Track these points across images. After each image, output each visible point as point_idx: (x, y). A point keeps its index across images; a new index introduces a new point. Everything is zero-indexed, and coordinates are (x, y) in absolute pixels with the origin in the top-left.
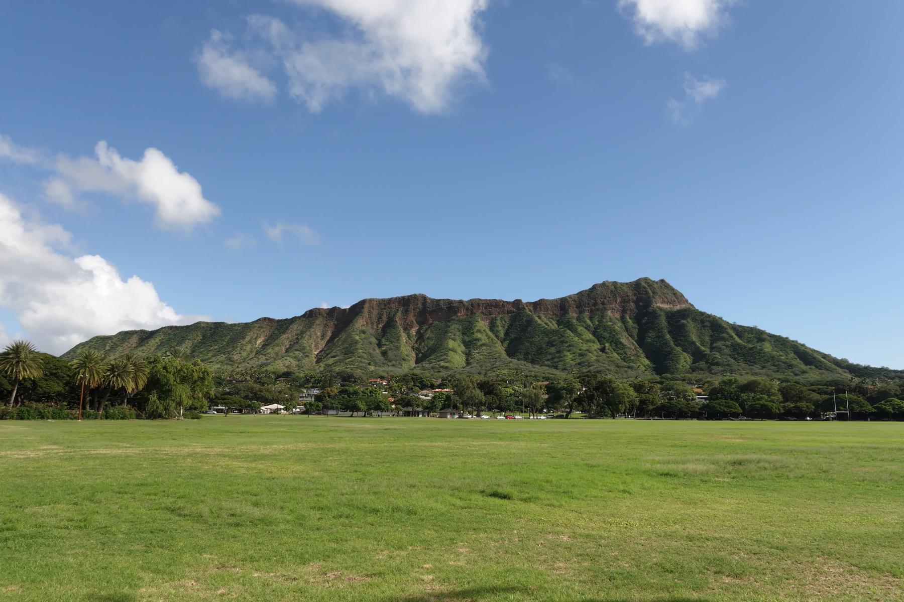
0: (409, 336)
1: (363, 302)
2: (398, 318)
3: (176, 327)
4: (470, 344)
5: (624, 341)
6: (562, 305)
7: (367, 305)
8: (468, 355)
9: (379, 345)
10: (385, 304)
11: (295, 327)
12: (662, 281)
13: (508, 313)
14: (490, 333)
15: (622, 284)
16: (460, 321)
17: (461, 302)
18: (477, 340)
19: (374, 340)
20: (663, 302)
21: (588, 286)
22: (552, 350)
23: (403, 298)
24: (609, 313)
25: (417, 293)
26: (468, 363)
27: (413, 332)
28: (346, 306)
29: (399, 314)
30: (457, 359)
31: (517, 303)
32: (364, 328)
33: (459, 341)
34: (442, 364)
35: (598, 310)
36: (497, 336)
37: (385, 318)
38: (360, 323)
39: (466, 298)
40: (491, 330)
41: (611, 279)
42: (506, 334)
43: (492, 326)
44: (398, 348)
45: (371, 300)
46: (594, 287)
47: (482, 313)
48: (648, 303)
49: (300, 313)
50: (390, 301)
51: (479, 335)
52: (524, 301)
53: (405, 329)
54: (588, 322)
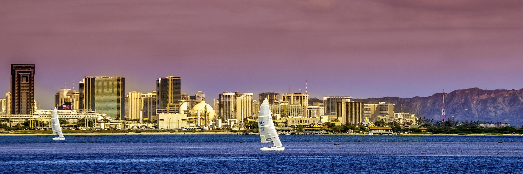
1: (455, 91)
4: (496, 108)
8: (495, 113)
17: (492, 91)
23: (470, 89)
31: (513, 90)
42: (509, 103)
44: (472, 110)
45: (458, 90)
49: (431, 95)
50: (466, 90)
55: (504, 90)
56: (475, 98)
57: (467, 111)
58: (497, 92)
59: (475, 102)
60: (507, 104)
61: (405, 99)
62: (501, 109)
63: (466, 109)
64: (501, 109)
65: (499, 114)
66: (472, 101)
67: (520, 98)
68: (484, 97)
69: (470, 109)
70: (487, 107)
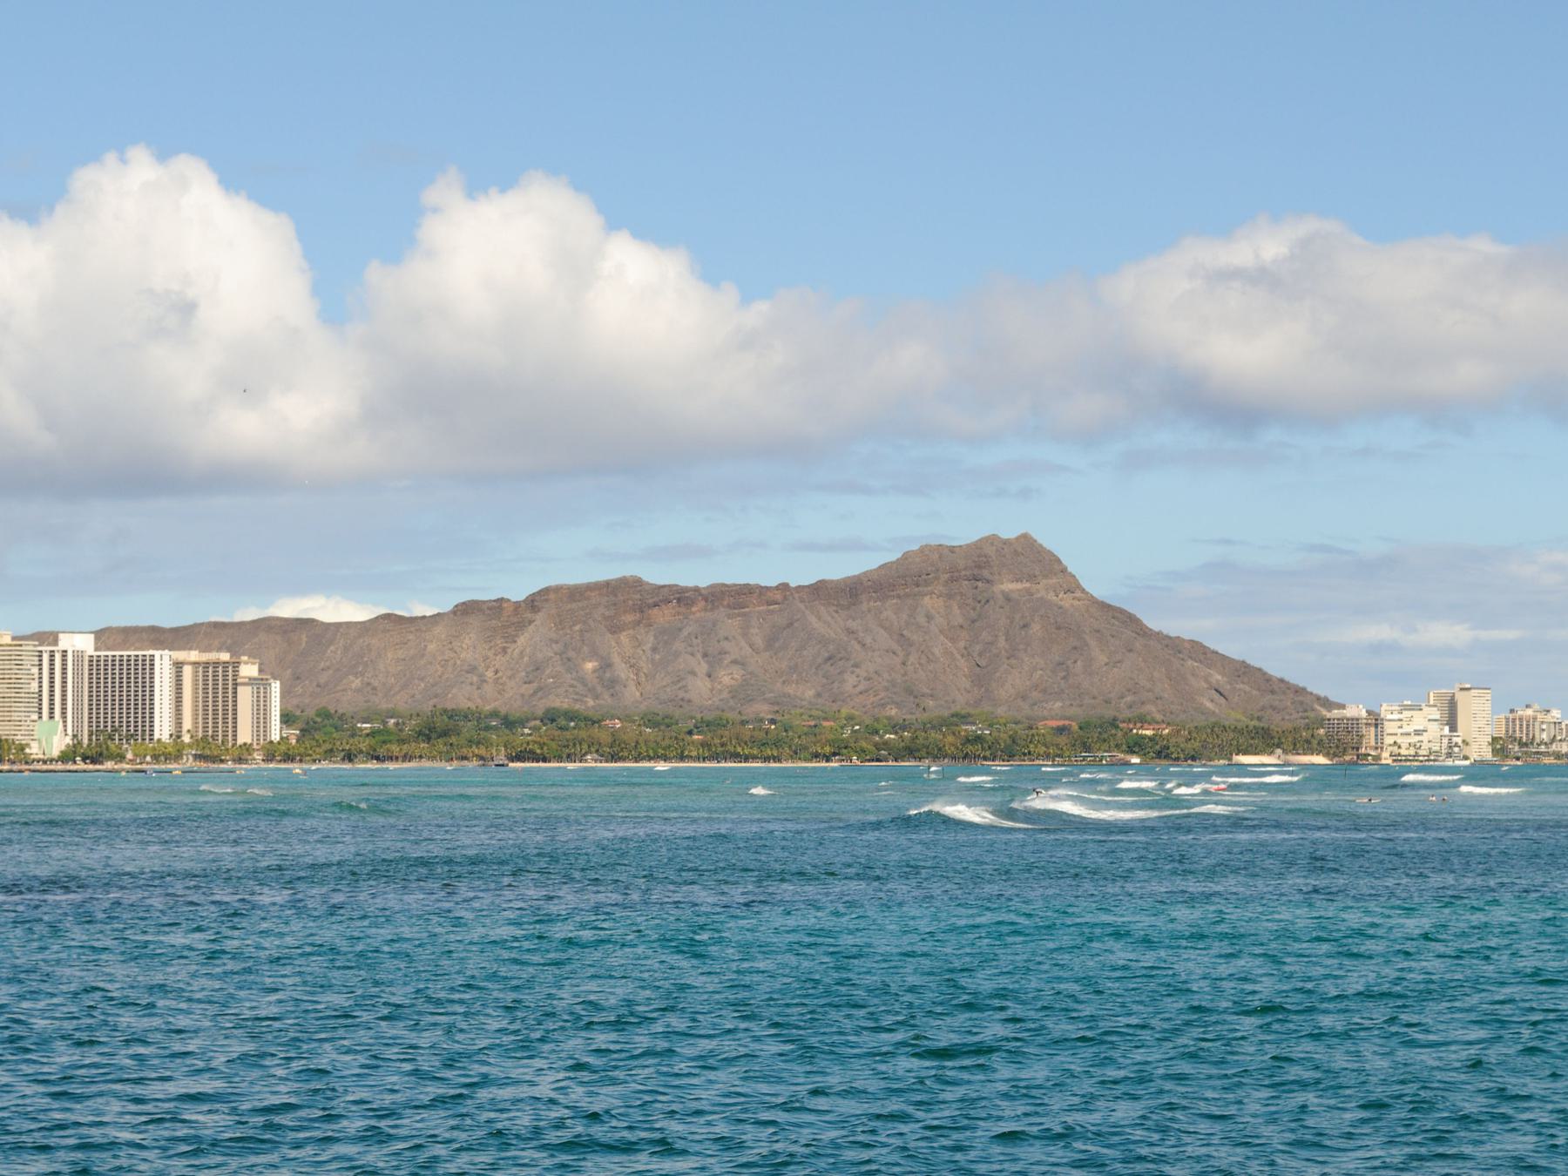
1: (545, 591)
4: (714, 660)
7: (552, 596)
10: (576, 593)
12: (1025, 537)
13: (769, 604)
14: (743, 643)
15: (952, 549)
17: (696, 590)
18: (723, 652)
23: (607, 584)
24: (927, 599)
31: (784, 587)
32: (553, 636)
33: (699, 656)
34: (681, 694)
35: (907, 595)
40: (745, 635)
42: (770, 642)
45: (557, 589)
47: (729, 606)
51: (725, 644)
52: (793, 585)
53: (613, 633)
56: (629, 618)
57: (594, 671)
59: (624, 637)
60: (759, 641)
61: (340, 624)
62: (735, 662)
63: (589, 666)
64: (735, 662)
65: (726, 680)
66: (615, 630)
67: (813, 619)
69: (606, 665)
70: (677, 655)
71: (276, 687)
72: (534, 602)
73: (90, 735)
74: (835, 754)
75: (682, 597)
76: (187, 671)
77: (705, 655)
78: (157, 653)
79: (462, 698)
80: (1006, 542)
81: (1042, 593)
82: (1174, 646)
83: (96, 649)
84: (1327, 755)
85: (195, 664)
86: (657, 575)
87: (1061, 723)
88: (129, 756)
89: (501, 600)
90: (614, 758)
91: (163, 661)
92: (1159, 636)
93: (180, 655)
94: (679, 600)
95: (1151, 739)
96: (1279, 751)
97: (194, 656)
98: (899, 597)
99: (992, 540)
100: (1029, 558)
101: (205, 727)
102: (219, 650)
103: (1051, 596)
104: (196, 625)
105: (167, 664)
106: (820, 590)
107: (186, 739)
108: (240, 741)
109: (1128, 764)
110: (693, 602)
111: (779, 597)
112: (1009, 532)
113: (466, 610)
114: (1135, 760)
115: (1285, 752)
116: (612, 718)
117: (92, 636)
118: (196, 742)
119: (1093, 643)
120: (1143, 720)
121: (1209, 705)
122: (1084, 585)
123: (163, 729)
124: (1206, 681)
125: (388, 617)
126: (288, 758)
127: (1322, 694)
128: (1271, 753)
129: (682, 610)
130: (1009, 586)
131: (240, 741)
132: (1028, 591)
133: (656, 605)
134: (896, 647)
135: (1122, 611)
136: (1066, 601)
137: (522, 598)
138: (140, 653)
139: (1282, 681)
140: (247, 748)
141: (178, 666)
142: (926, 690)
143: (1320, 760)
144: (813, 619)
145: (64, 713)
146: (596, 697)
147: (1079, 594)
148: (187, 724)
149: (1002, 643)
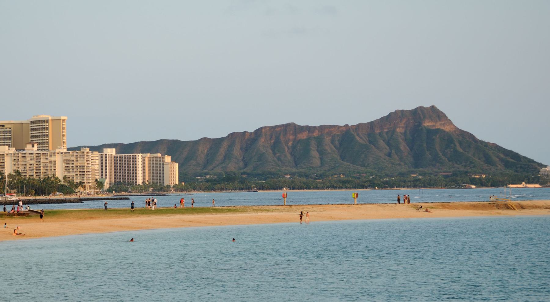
0: (288, 147)
1: (262, 128)
2: (281, 137)
3: (146, 142)
4: (322, 152)
5: (402, 148)
6: (371, 125)
7: (263, 130)
8: (321, 159)
9: (274, 154)
10: (273, 128)
11: (225, 144)
12: (433, 107)
14: (333, 146)
15: (406, 111)
16: (315, 138)
17: (315, 127)
19: (271, 151)
20: (429, 122)
21: (386, 114)
22: (363, 156)
23: (283, 125)
24: (398, 130)
25: (290, 122)
26: (322, 164)
27: (290, 144)
28: (251, 130)
29: (282, 134)
30: (317, 162)
31: (347, 125)
36: (335, 147)
37: (274, 137)
38: (262, 140)
39: (318, 125)
41: (401, 108)
43: (332, 142)
45: (265, 127)
46: (390, 114)
48: (420, 124)
50: (276, 127)
52: (350, 125)
54: (386, 136)
55: (333, 126)
56: (291, 137)
58: (322, 128)
62: (329, 153)
66: (286, 143)
67: (357, 138)
68: (303, 136)
71: (177, 165)
72: (258, 132)
73: (115, 182)
74: (369, 186)
75: (309, 129)
76: (146, 159)
77: (318, 151)
78: (137, 155)
79: (232, 167)
80: (426, 109)
81: (439, 127)
82: (486, 144)
83: (116, 154)
84: (540, 184)
85: (149, 158)
86: (301, 122)
87: (447, 173)
88: (130, 190)
89: (245, 132)
90: (294, 188)
91: (139, 157)
92: (482, 142)
93: (144, 155)
94: (309, 132)
95: (478, 178)
96: (524, 183)
97: (148, 154)
98: (388, 129)
99: (421, 108)
100: (435, 113)
101: (153, 178)
102: (157, 152)
103: (442, 128)
104: (136, 143)
105: (140, 156)
106: (359, 126)
107: (147, 183)
108: (166, 184)
109: (471, 188)
110: (314, 132)
111: (344, 129)
112: (427, 105)
113: (233, 136)
114: (474, 187)
115: (526, 183)
116: (287, 174)
117: (114, 150)
118: (151, 185)
119: (457, 145)
120: (476, 173)
121: (499, 166)
122: (454, 123)
123: (140, 181)
124: (498, 157)
125: (205, 138)
126: (182, 190)
127: (540, 162)
128: (521, 183)
129: (310, 134)
130: (427, 124)
131: (166, 184)
132: (434, 126)
133: (300, 133)
134: (387, 147)
135: (468, 133)
136: (447, 128)
137: (252, 131)
138: (131, 155)
139: (525, 157)
140: (168, 187)
141: (144, 159)
142: (398, 163)
143: (537, 186)
144: (357, 138)
145: (106, 174)
146: (279, 166)
147: (452, 127)
148: (147, 179)
149: (425, 145)
